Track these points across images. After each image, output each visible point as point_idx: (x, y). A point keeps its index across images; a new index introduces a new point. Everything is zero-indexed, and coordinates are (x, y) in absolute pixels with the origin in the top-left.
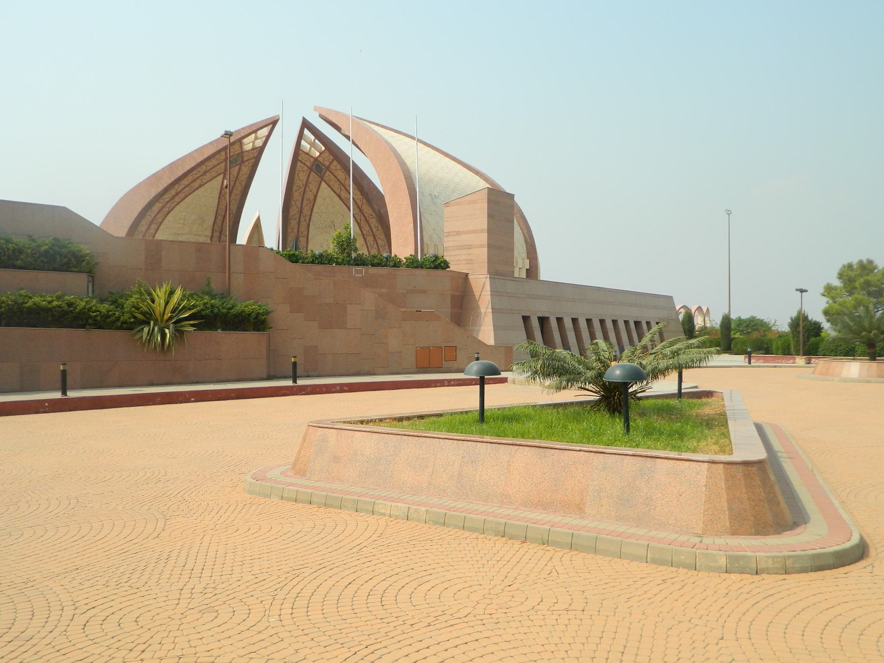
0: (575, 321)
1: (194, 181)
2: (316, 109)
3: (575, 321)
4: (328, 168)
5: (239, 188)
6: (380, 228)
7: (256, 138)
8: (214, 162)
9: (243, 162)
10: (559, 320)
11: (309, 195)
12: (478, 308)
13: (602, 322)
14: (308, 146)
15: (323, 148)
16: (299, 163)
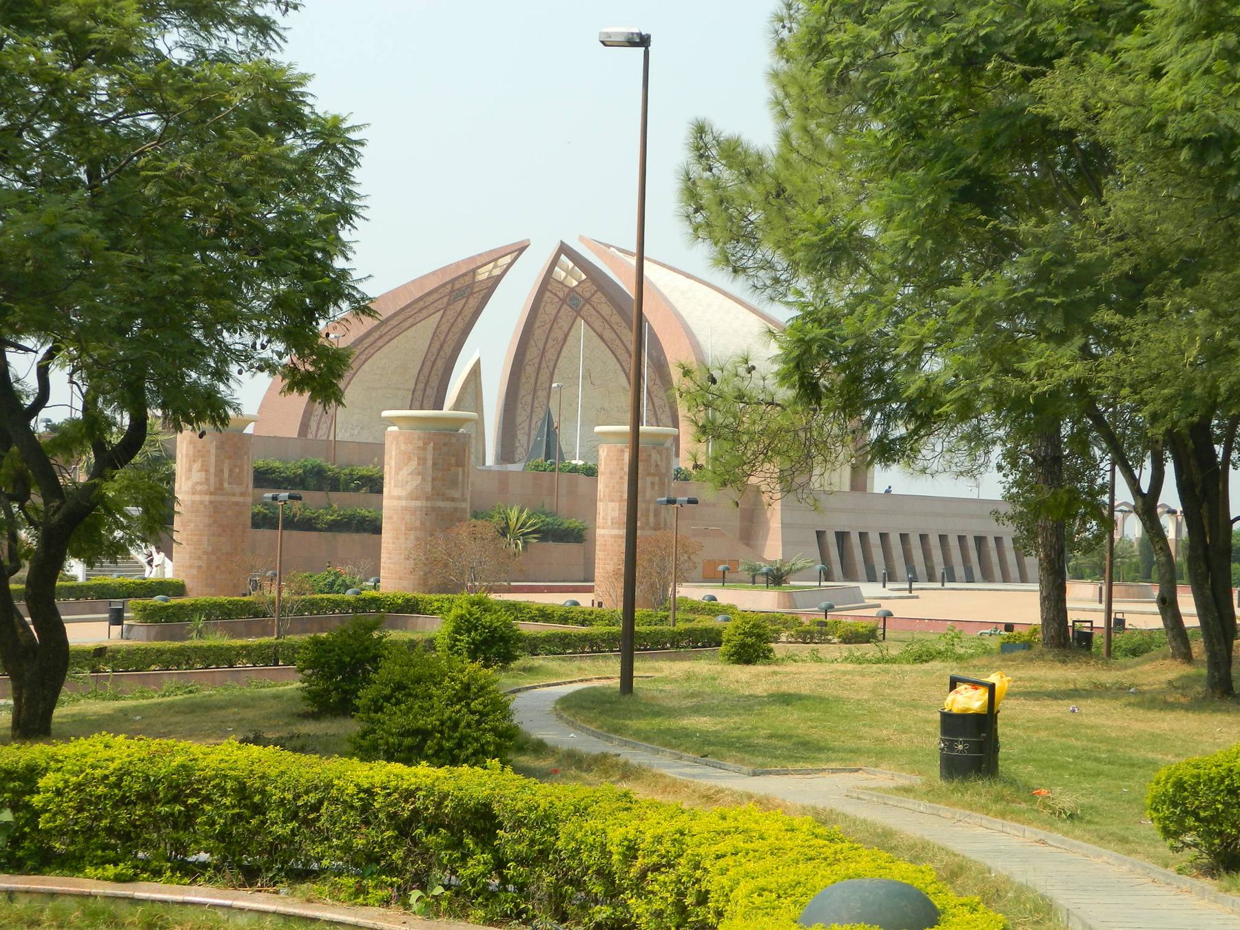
0: (884, 537)
1: (405, 320)
2: (581, 239)
3: (884, 537)
4: (588, 301)
5: (460, 324)
6: (658, 381)
7: (495, 267)
8: (436, 296)
9: (472, 294)
10: (863, 536)
11: (558, 334)
12: (767, 522)
13: (923, 538)
14: (563, 274)
15: (584, 277)
16: (548, 294)
